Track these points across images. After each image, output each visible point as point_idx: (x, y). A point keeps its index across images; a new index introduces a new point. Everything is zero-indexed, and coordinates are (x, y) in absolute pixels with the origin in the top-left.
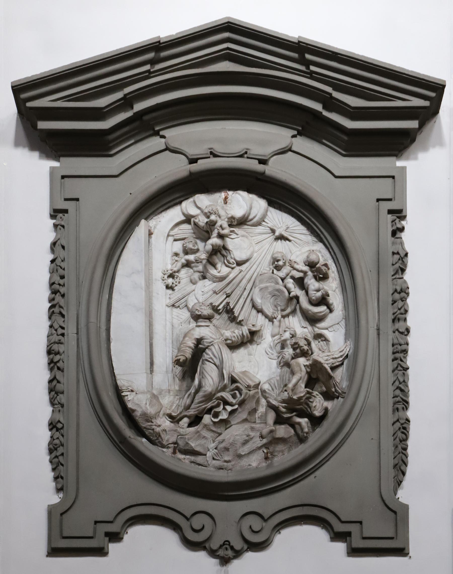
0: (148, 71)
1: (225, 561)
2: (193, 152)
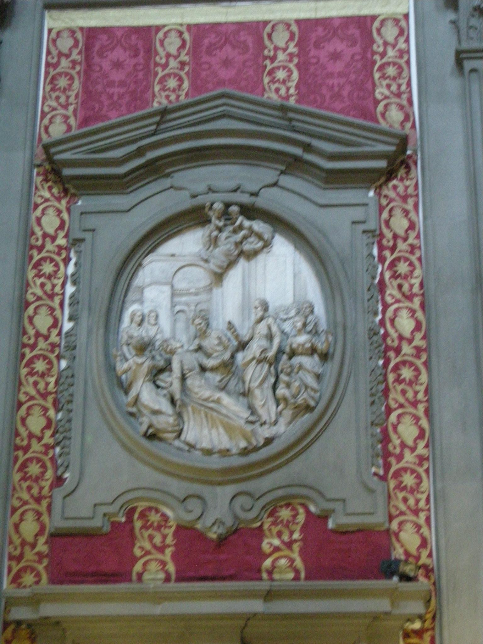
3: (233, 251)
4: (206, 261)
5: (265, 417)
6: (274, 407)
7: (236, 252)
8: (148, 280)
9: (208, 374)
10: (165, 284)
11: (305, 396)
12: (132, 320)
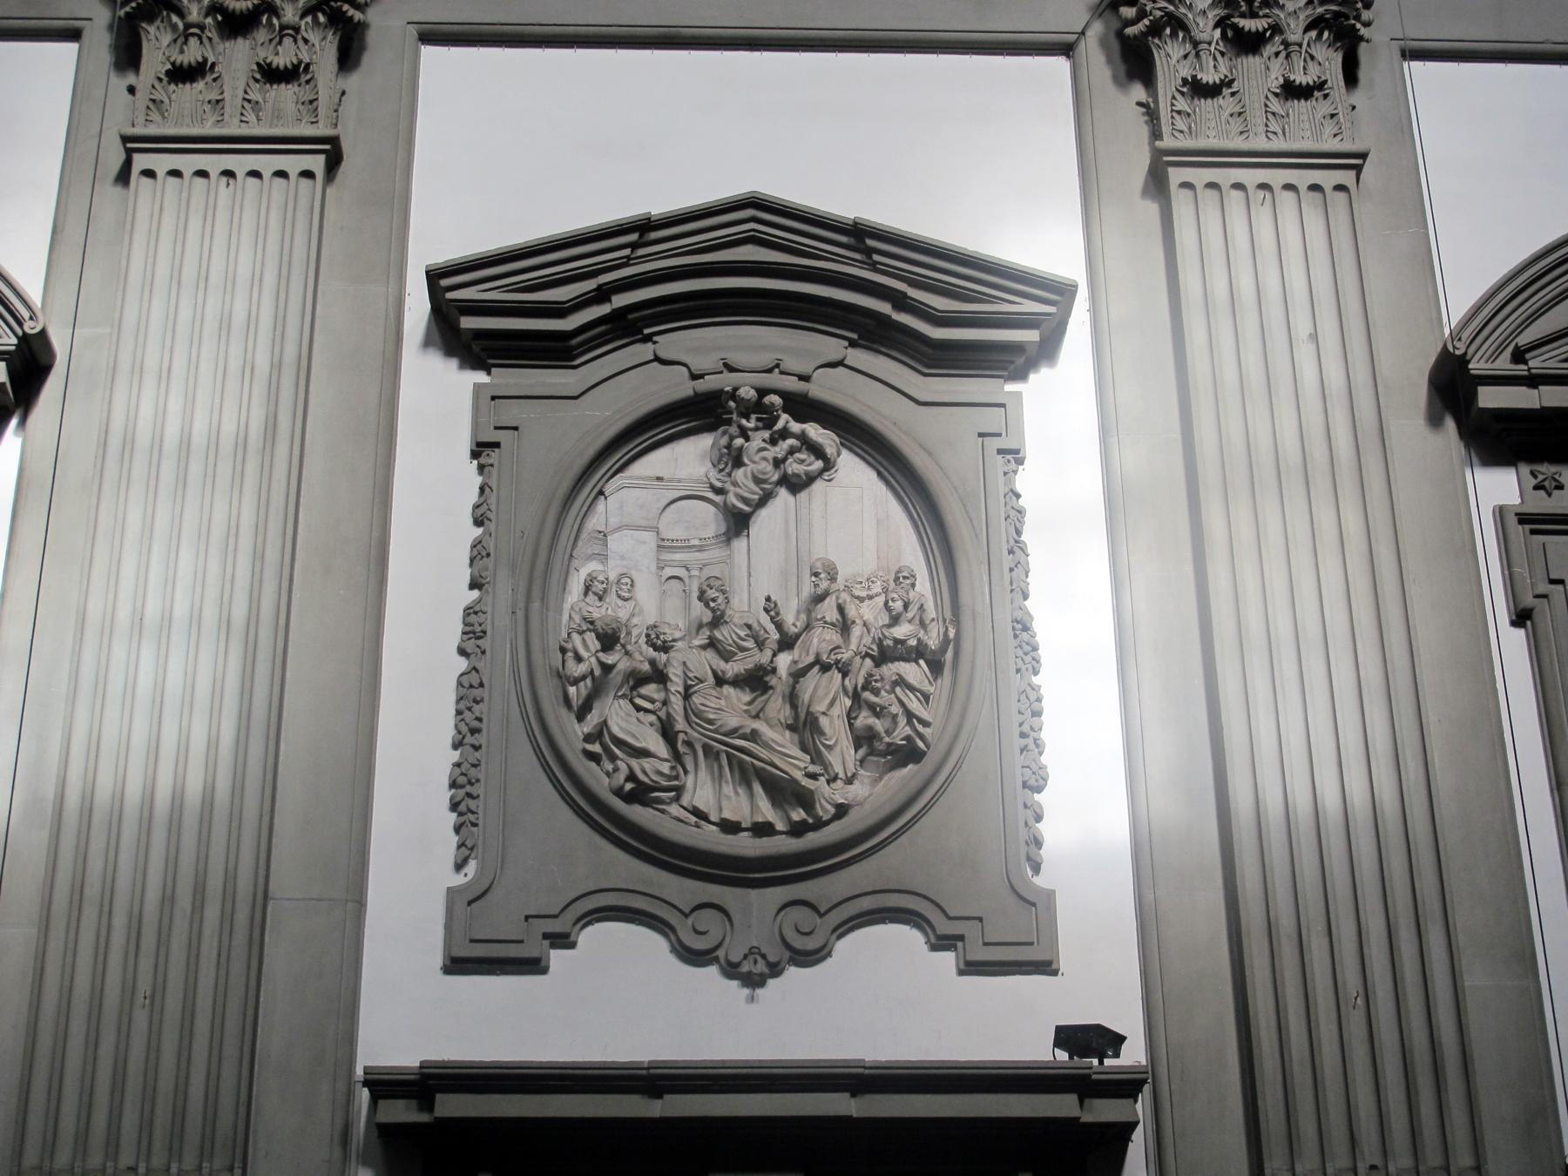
0: (629, 258)
1: (754, 982)
2: (698, 364)
3: (771, 474)
4: (719, 491)
5: (839, 769)
6: (853, 752)
7: (775, 478)
8: (614, 521)
9: (727, 690)
10: (645, 529)
11: (908, 731)
12: (587, 589)
